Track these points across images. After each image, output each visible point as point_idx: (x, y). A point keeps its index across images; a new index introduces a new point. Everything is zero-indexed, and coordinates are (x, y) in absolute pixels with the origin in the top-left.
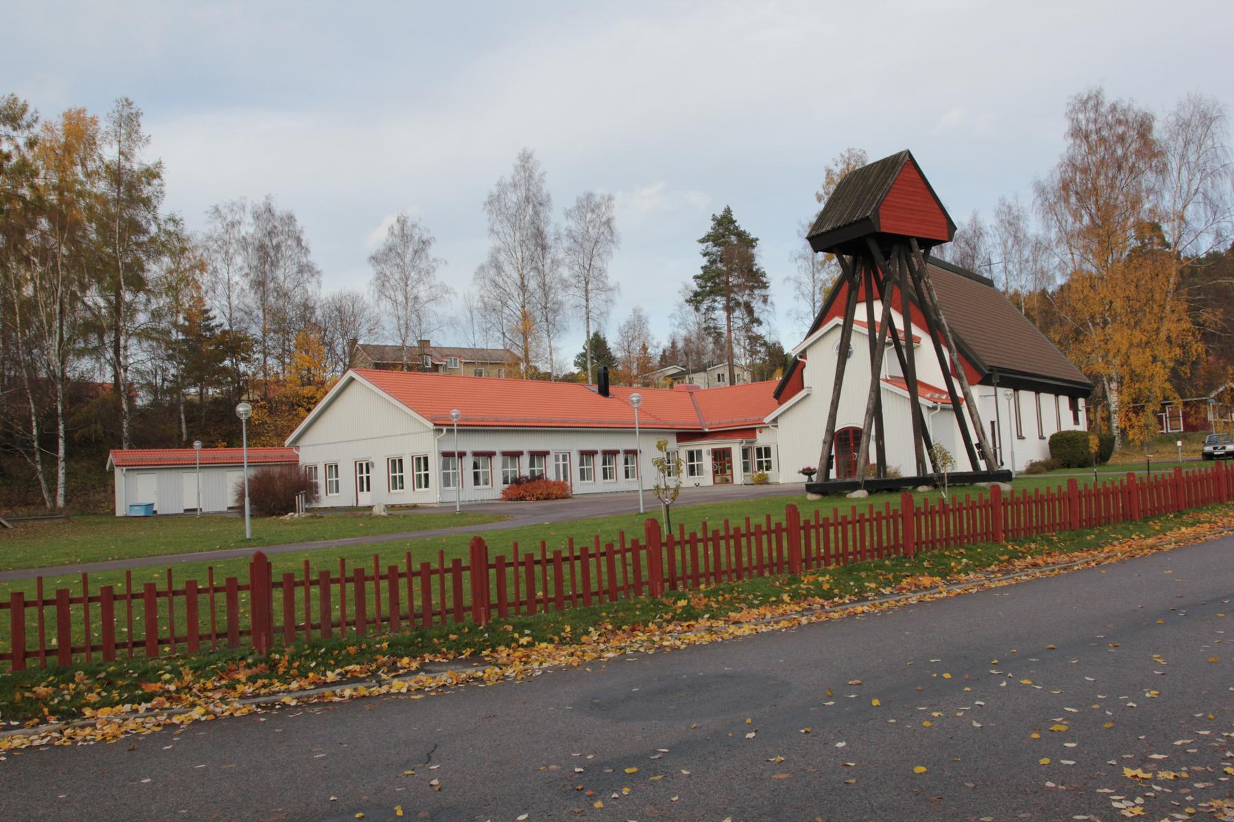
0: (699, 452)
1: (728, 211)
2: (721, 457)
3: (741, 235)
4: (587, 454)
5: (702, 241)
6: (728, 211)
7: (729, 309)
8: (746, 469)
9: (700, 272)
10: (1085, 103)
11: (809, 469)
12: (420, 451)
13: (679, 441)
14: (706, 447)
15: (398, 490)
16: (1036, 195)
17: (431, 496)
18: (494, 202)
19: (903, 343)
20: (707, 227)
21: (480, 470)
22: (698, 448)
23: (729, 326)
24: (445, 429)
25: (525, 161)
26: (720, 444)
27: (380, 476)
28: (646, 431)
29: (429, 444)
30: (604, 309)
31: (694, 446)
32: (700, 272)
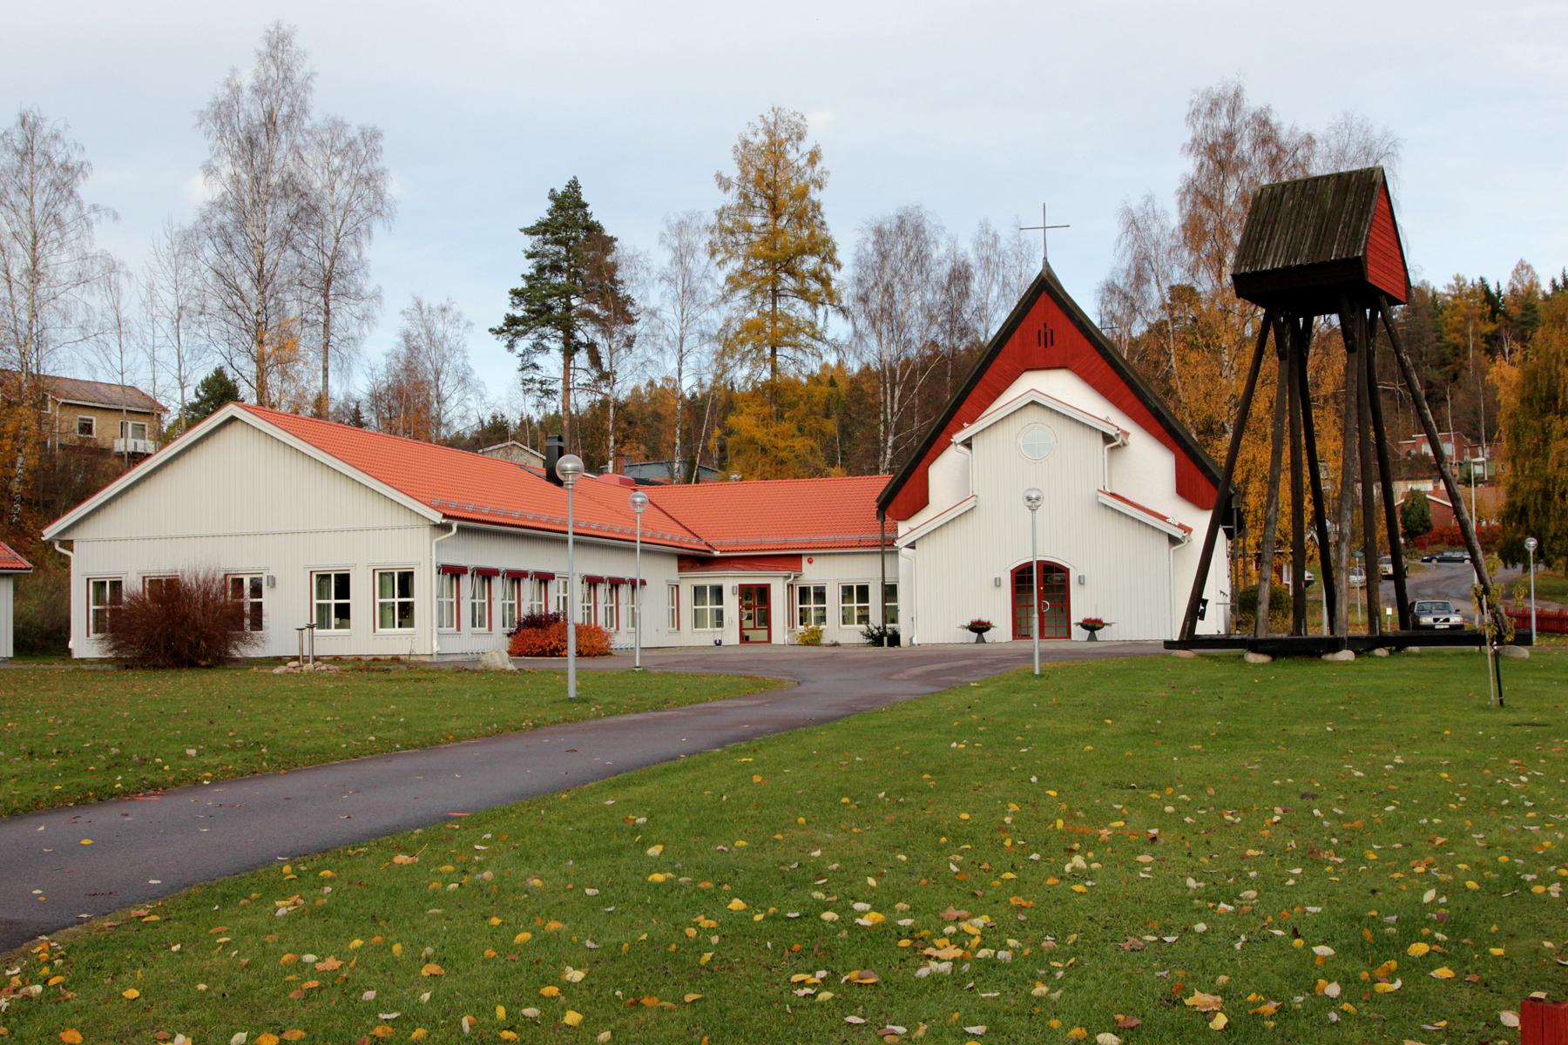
0: (718, 592)
1: (574, 186)
2: (756, 598)
3: (593, 229)
4: (593, 582)
5: (530, 232)
6: (574, 186)
7: (569, 350)
8: (791, 623)
9: (521, 284)
10: (1216, 104)
11: (979, 623)
12: (397, 561)
13: (680, 569)
14: (730, 582)
15: (333, 631)
16: (1123, 228)
17: (422, 639)
18: (222, 114)
19: (1287, 440)
20: (541, 210)
21: (333, 601)
22: (716, 582)
23: (566, 381)
24: (455, 524)
25: (277, 45)
26: (754, 578)
27: (362, 598)
28: (653, 550)
29: (420, 552)
30: (354, 331)
31: (708, 579)
32: (521, 284)
